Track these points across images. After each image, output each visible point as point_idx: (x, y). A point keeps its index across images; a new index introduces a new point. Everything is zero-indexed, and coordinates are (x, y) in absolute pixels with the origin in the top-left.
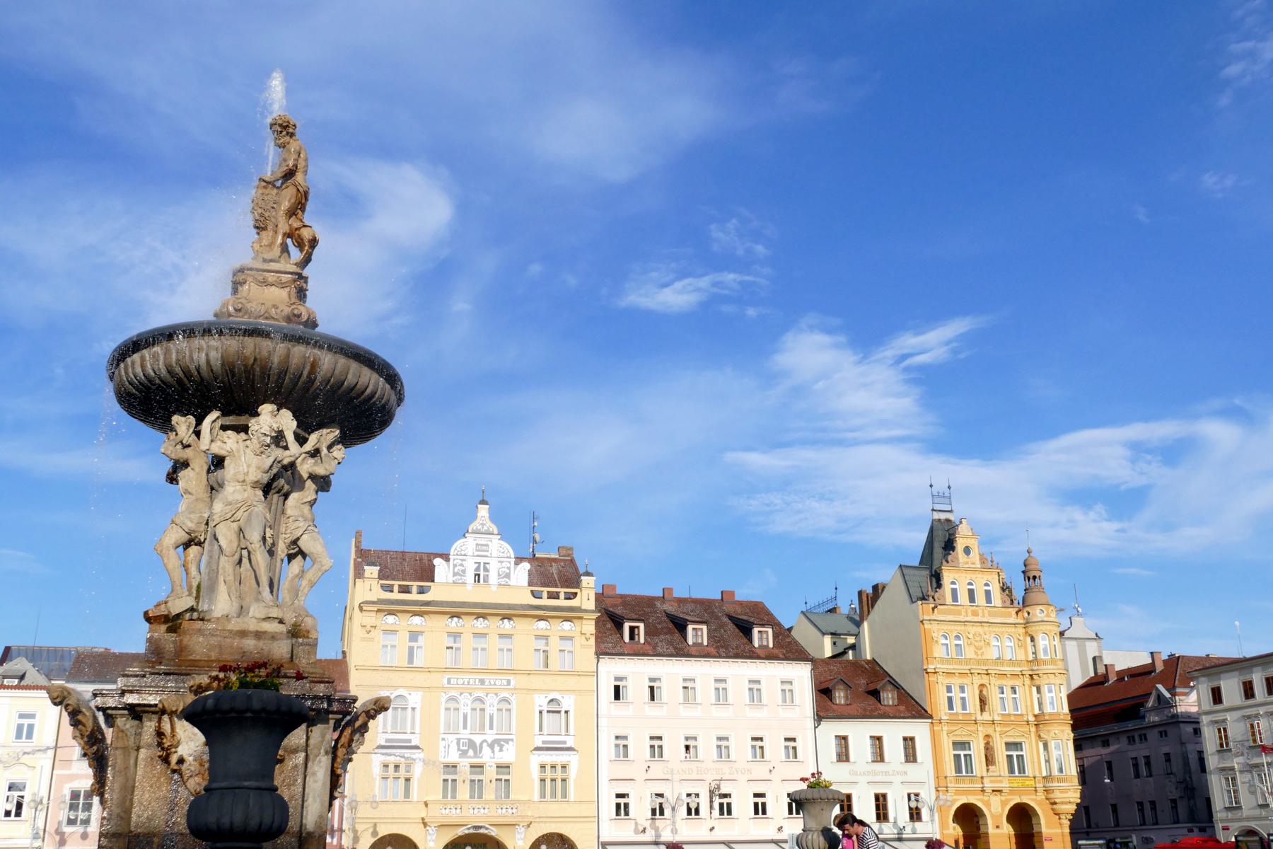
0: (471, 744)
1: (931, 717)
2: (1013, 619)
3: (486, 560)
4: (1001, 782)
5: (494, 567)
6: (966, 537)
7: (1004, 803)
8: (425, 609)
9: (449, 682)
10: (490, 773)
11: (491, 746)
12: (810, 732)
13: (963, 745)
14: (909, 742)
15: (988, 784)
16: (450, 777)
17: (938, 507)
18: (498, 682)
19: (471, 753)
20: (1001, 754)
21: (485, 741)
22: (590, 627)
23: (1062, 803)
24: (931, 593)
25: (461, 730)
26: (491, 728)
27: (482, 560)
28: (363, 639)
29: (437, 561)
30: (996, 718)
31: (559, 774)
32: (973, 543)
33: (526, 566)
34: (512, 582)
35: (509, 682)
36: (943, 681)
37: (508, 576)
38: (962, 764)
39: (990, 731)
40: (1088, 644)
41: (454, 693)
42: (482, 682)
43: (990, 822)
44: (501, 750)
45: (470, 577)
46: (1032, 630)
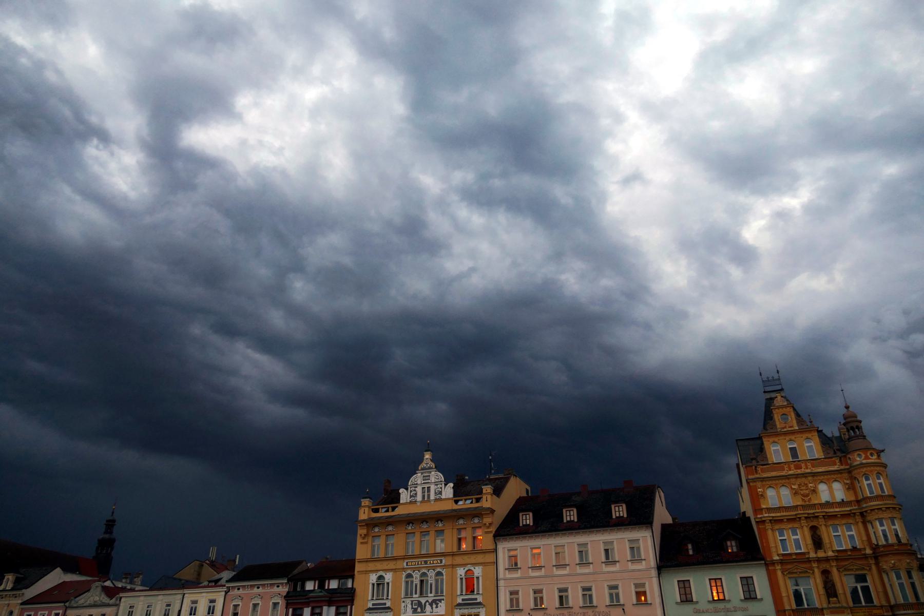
0: (420, 604)
1: (763, 559)
2: (836, 468)
5: (433, 488)
11: (431, 605)
12: (655, 581)
14: (747, 582)
17: (768, 389)
19: (419, 610)
28: (362, 543)
29: (401, 491)
30: (830, 554)
33: (451, 485)
34: (443, 497)
35: (441, 561)
37: (440, 493)
39: (825, 566)
42: (426, 562)
45: (419, 498)
46: (855, 473)
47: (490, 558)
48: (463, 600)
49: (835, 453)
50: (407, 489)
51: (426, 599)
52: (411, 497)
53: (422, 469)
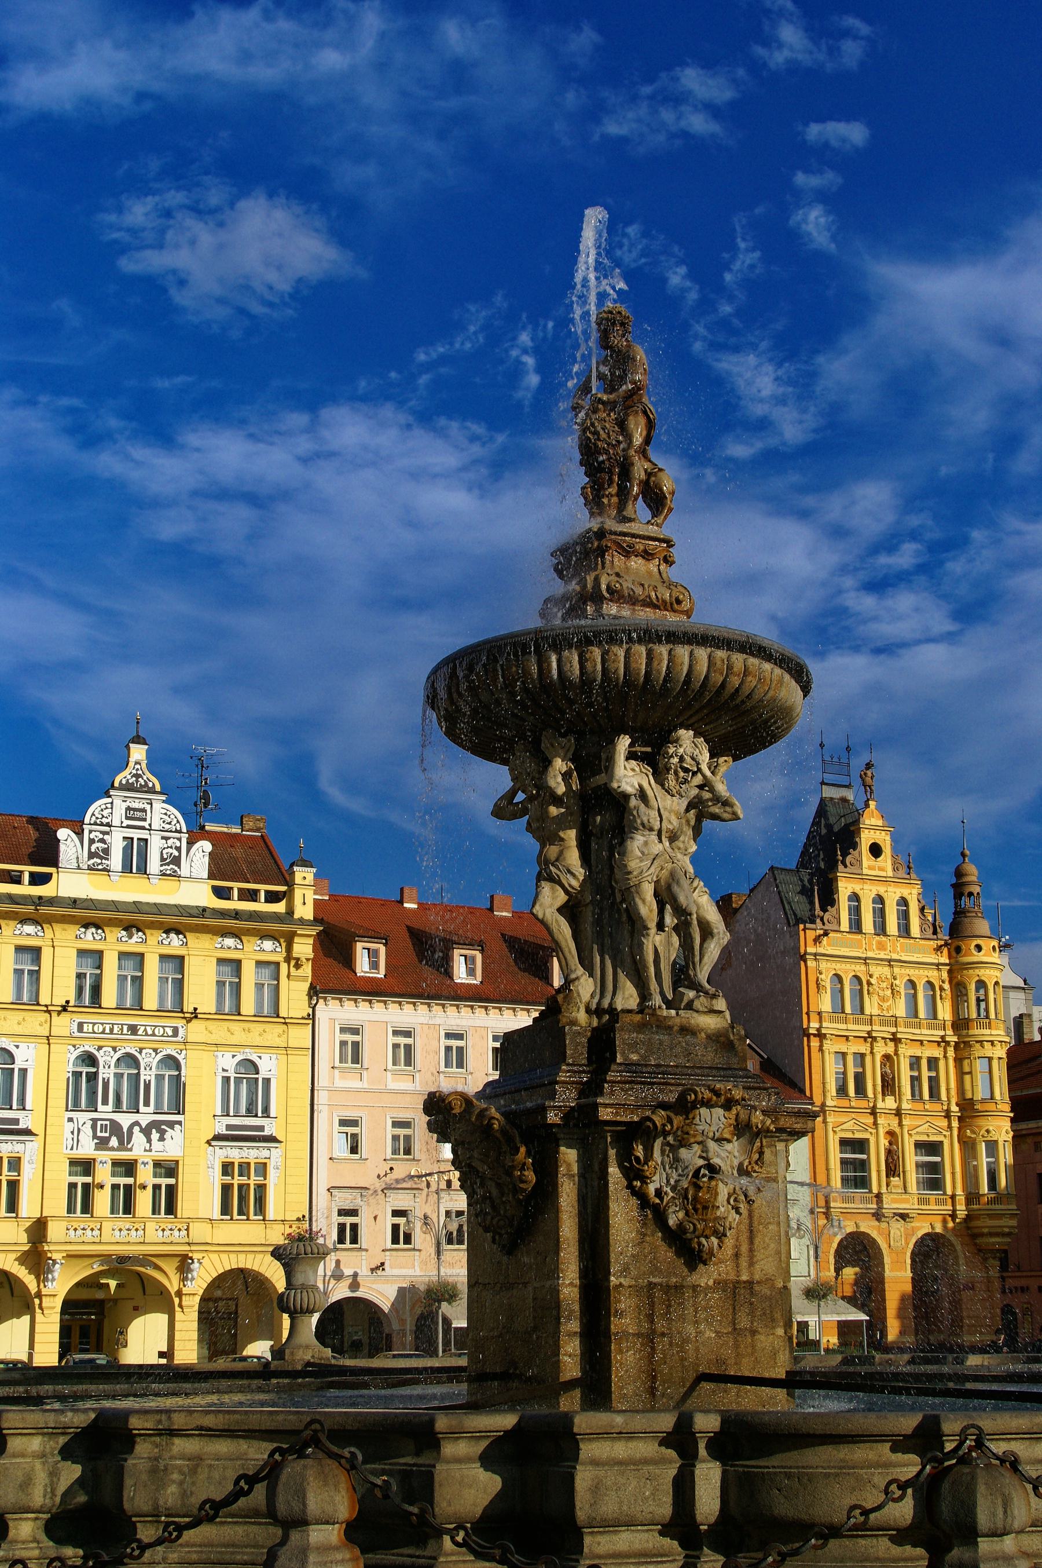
0: (115, 1128)
2: (933, 958)
3: (144, 834)
4: (907, 1201)
5: (156, 845)
6: (874, 828)
7: (908, 1236)
8: (40, 913)
9: (80, 1026)
10: (145, 1175)
11: (146, 1132)
13: (859, 1145)
15: (890, 1204)
16: (81, 1180)
17: (829, 778)
18: (159, 1031)
19: (114, 1142)
20: (911, 1159)
21: (137, 1123)
22: (304, 948)
23: (991, 1235)
24: (818, 911)
25: (142, 1109)
26: (147, 1103)
27: (136, 834)
29: (63, 833)
31: (254, 1180)
32: (884, 840)
33: (206, 846)
35: (176, 1031)
36: (830, 1046)
37: (176, 861)
38: (856, 1175)
40: (1012, 994)
41: (89, 1047)
43: (887, 1260)
44: (162, 1139)
45: (116, 860)
47: (301, 1036)
48: (229, 1127)
49: (935, 933)
50: (80, 833)
51: (134, 1117)
52: (92, 855)
53: (128, 787)
